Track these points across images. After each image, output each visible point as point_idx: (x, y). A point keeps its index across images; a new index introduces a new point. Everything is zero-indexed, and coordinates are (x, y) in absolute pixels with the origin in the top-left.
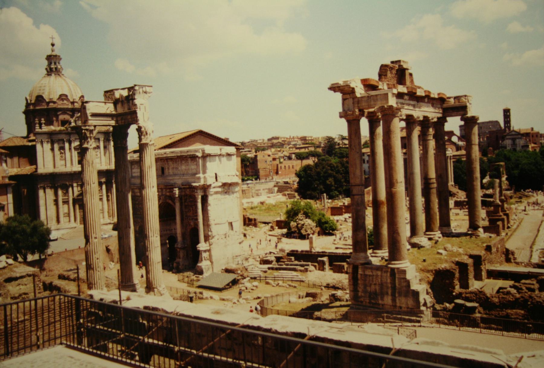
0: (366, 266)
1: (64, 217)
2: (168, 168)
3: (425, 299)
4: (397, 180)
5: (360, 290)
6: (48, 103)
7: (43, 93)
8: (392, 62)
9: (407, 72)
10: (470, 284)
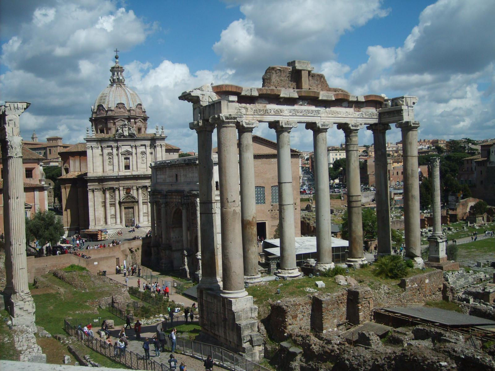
0: (209, 292)
1: (111, 218)
2: (180, 175)
3: (251, 336)
4: (227, 199)
5: (205, 317)
6: (107, 111)
7: (104, 103)
8: (289, 64)
9: (304, 75)
10: (325, 325)
